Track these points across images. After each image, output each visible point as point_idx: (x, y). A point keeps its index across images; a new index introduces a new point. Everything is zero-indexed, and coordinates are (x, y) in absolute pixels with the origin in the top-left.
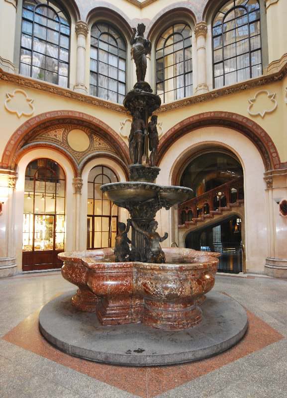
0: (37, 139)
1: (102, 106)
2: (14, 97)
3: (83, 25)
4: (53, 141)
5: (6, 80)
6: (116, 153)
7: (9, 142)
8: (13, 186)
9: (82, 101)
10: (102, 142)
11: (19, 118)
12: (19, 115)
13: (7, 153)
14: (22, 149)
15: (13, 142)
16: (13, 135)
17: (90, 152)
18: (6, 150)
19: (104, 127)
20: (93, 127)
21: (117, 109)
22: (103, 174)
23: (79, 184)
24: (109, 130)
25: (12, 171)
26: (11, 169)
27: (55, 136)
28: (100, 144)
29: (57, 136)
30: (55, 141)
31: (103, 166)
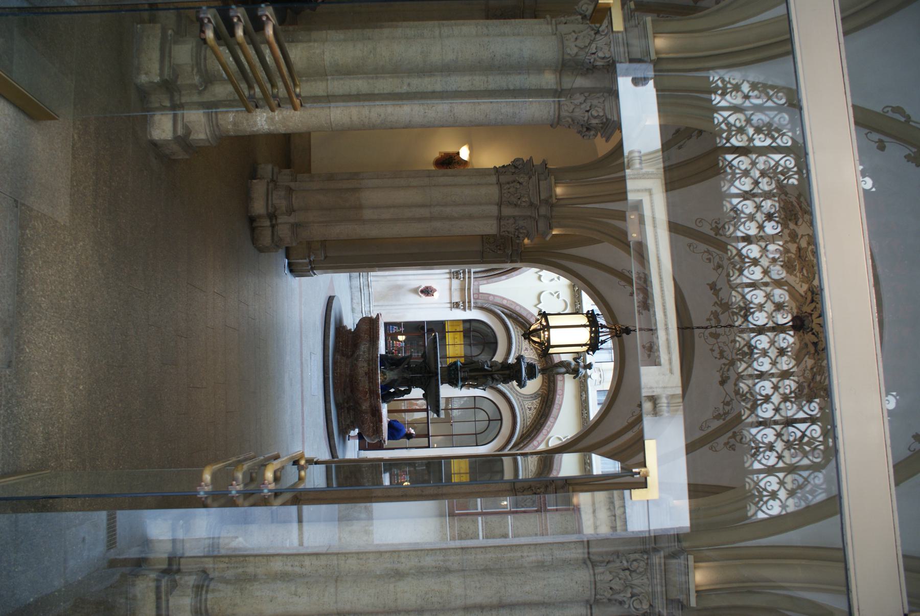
1: (582, 404)
4: (519, 346)
6: (521, 437)
7: (504, 299)
10: (534, 412)
11: (536, 306)
12: (538, 306)
13: (491, 298)
14: (500, 312)
15: (505, 302)
16: (513, 302)
17: (515, 395)
18: (494, 296)
19: (554, 411)
20: (551, 396)
22: (489, 420)
25: (472, 305)
26: (474, 303)
27: (526, 349)
28: (530, 409)
29: (526, 352)
30: (519, 349)
31: (501, 420)
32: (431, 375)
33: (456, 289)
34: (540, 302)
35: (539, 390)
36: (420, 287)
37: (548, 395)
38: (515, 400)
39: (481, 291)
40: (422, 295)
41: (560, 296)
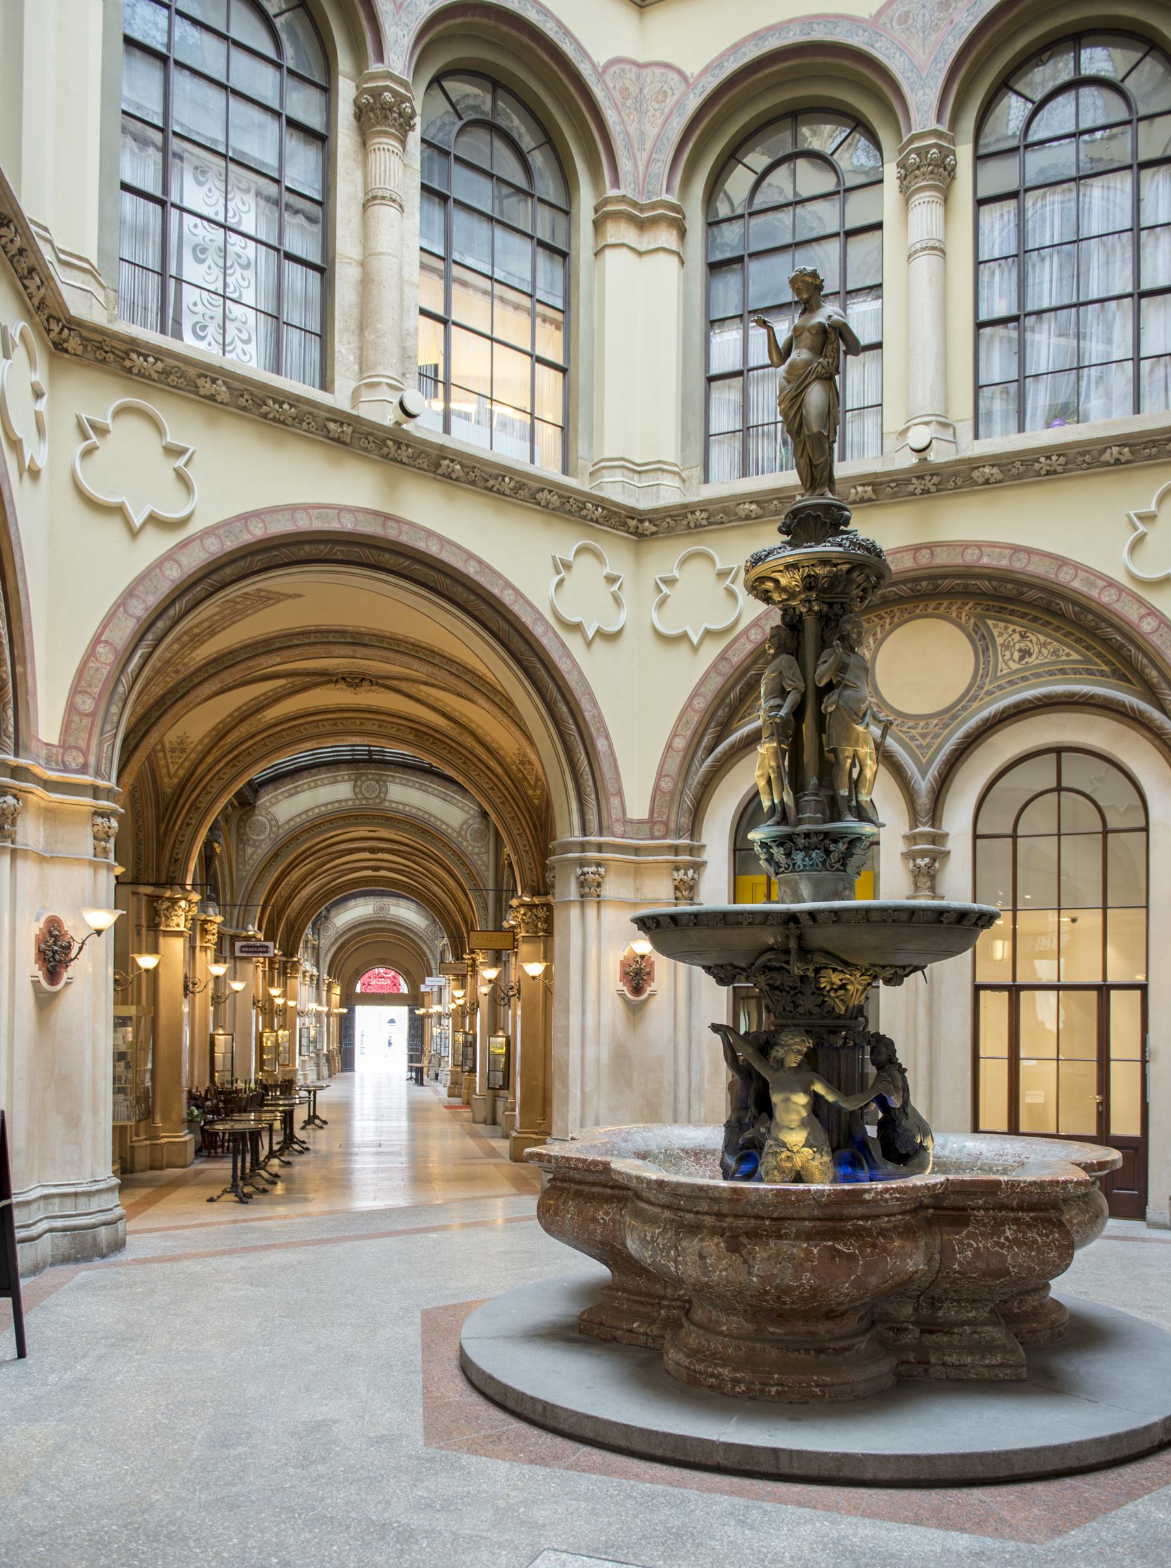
2: (678, 584)
3: (919, 152)
5: (652, 534)
8: (686, 893)
9: (926, 492)
12: (695, 639)
19: (1038, 568)
20: (985, 585)
21: (1106, 456)
23: (923, 854)
24: (1065, 577)
33: (637, 890)
35: (953, 622)
37: (984, 595)
38: (990, 703)
40: (648, 990)
41: (667, 575)
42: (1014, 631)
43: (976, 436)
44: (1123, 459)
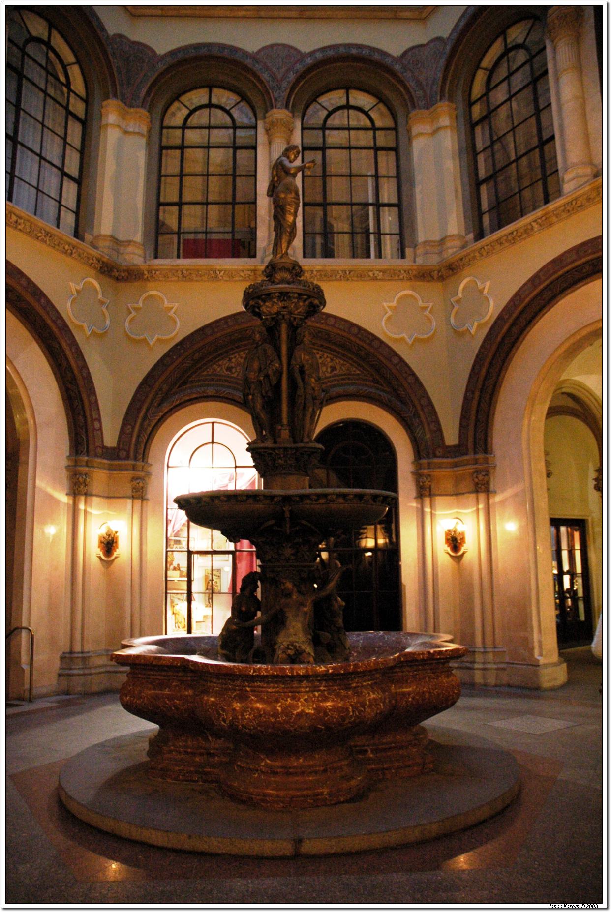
0: (192, 382)
12: (151, 343)
28: (333, 368)
32: (287, 515)
34: (145, 341)
36: (100, 558)
39: (114, 445)
40: (115, 554)
42: (327, 357)
43: (304, 257)
44: (379, 278)
